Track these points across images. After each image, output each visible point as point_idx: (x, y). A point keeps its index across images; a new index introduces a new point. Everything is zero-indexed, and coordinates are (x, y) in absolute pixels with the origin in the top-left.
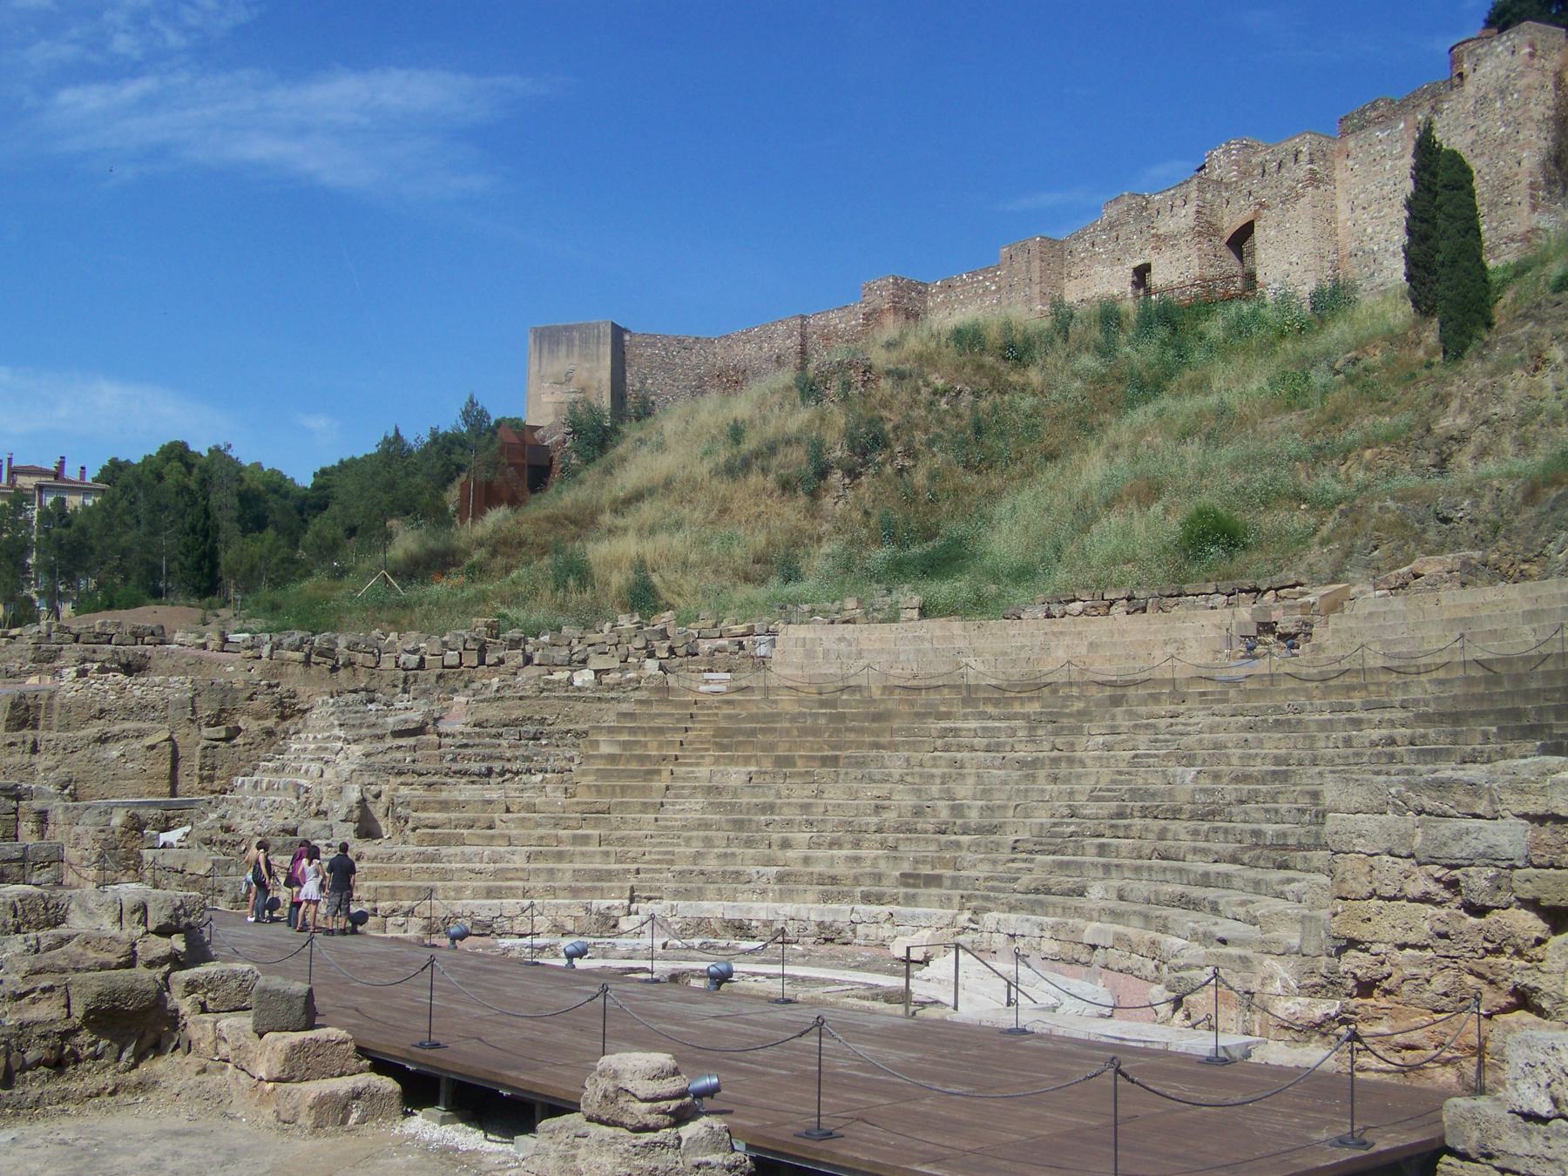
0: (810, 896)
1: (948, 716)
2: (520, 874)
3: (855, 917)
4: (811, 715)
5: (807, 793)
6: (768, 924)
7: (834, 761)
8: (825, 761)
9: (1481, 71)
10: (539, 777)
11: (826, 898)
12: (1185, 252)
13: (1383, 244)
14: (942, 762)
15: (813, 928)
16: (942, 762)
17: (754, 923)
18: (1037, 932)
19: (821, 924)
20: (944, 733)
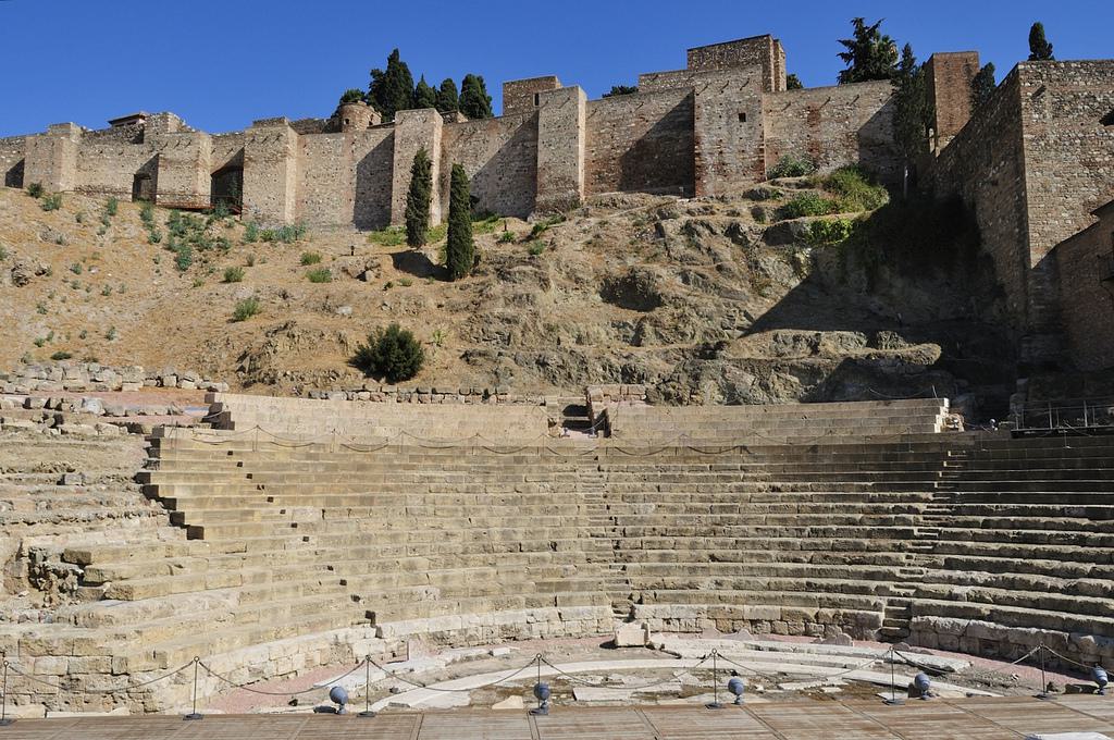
0: (486, 606)
1: (412, 468)
2: (253, 617)
3: (531, 619)
4: (312, 464)
5: (380, 526)
6: (463, 632)
7: (370, 501)
8: (363, 501)
9: (404, 125)
10: (136, 521)
11: (497, 606)
12: (187, 174)
13: (326, 200)
14: (449, 501)
15: (497, 631)
16: (449, 501)
17: (452, 633)
18: (693, 615)
19: (504, 628)
20: (423, 479)
